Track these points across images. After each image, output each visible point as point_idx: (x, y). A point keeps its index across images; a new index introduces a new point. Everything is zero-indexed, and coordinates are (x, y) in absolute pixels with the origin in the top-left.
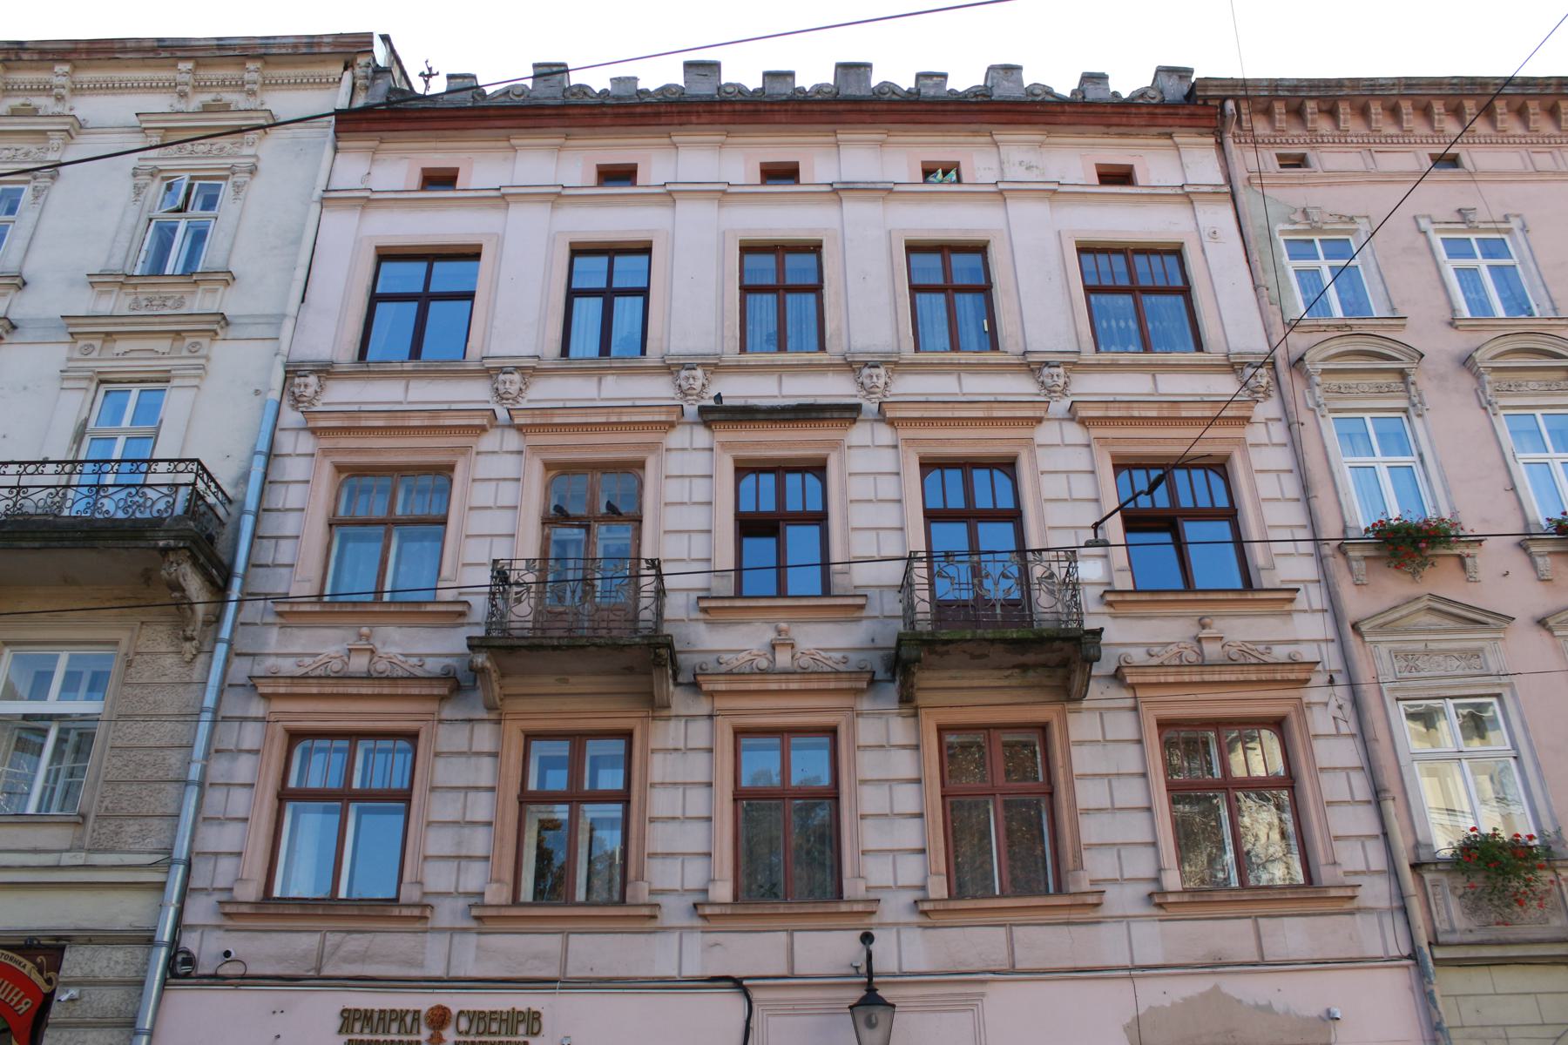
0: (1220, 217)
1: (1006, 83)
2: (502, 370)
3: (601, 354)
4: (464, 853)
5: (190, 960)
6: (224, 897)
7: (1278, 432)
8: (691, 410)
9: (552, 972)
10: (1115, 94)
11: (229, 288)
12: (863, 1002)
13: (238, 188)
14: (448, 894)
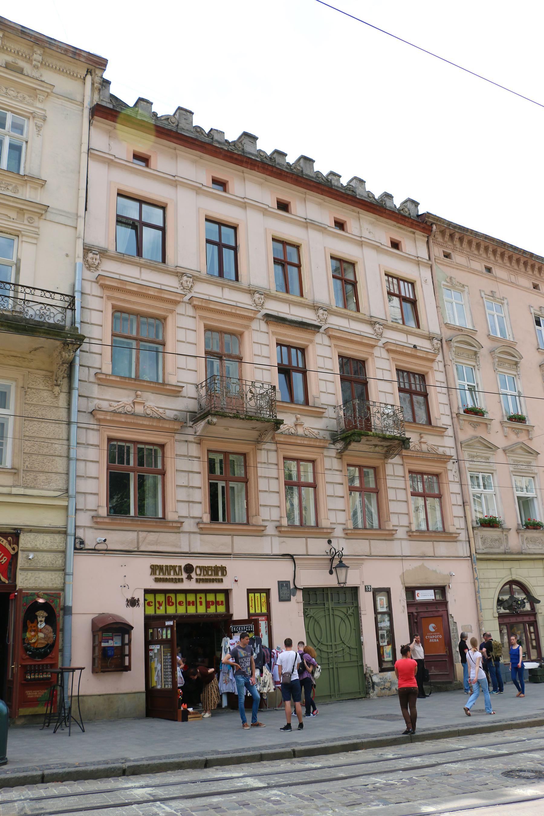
0: (426, 273)
2: (183, 274)
4: (191, 500)
5: (82, 542)
6: (93, 513)
9: (228, 551)
13: (39, 128)
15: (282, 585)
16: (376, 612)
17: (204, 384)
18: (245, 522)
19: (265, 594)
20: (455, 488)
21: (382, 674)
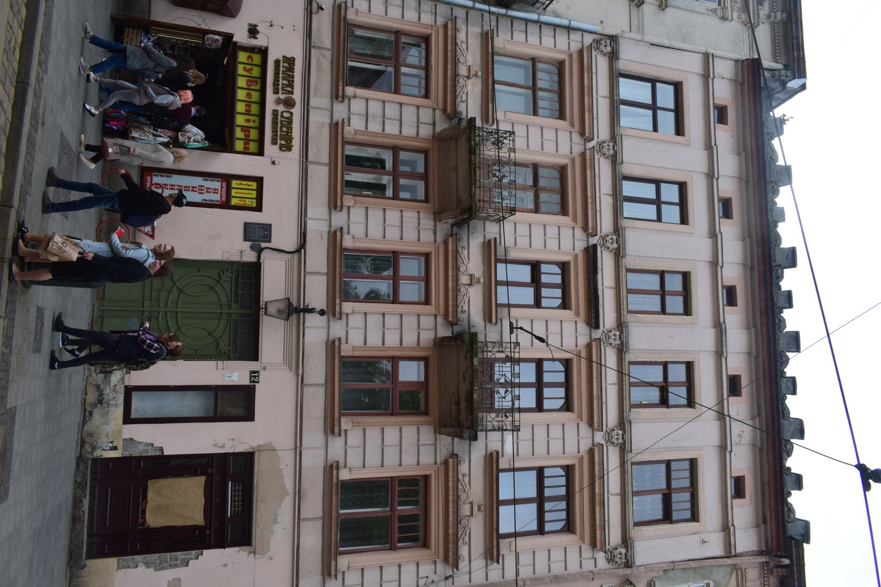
1: (792, 428)
3: (624, 196)
4: (369, 118)
7: (588, 565)
8: (593, 241)
10: (789, 494)
11: (657, 7)
12: (290, 304)
13: (714, 11)
14: (349, 110)
19: (254, 205)
21: (123, 390)
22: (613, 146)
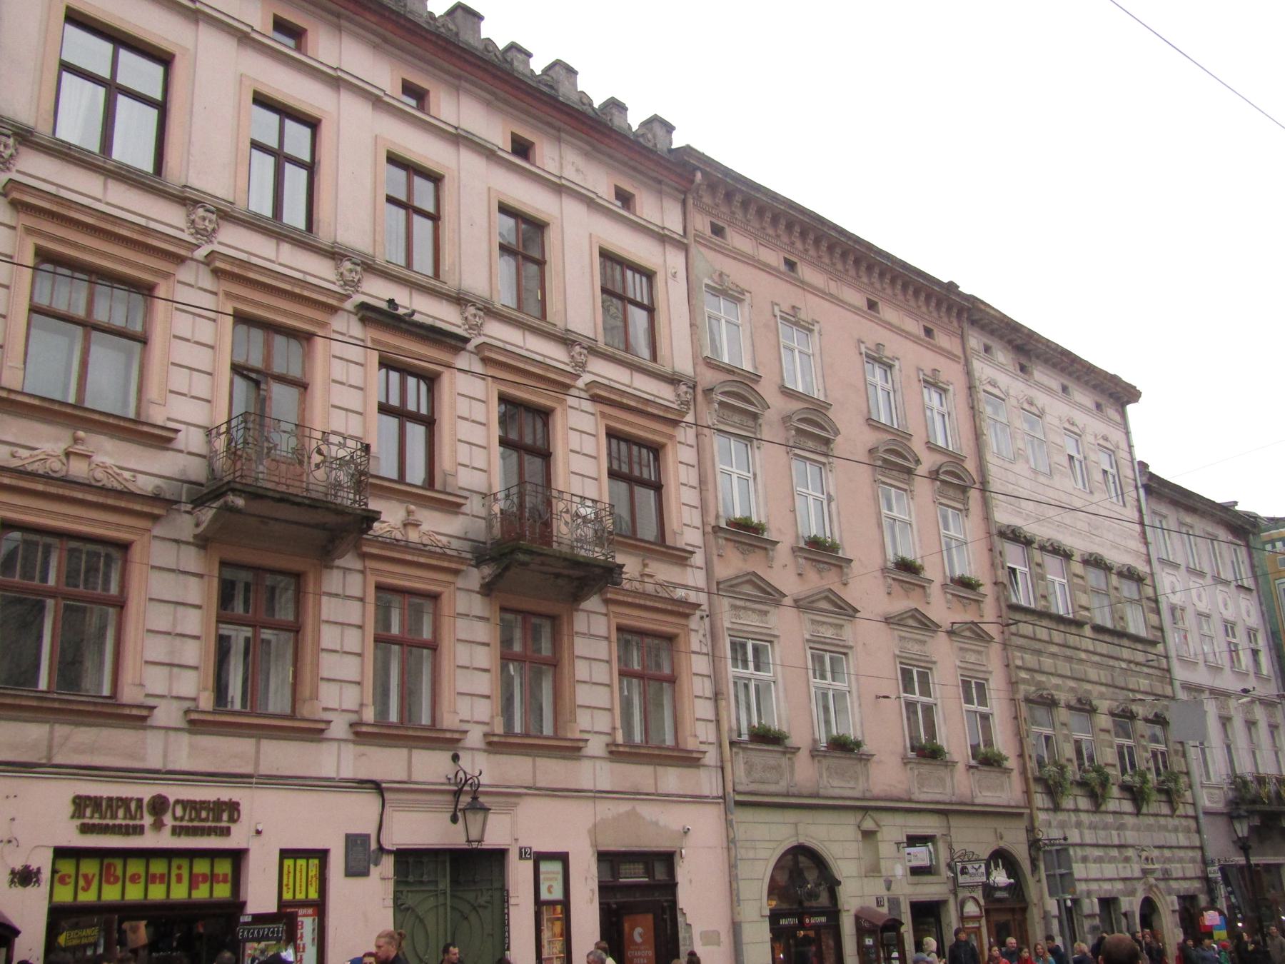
0: (676, 260)
2: (196, 203)
4: (176, 662)
15: (355, 842)
16: (539, 903)
17: (223, 428)
18: (288, 711)
19: (316, 861)
20: (700, 664)
22: (208, 211)
